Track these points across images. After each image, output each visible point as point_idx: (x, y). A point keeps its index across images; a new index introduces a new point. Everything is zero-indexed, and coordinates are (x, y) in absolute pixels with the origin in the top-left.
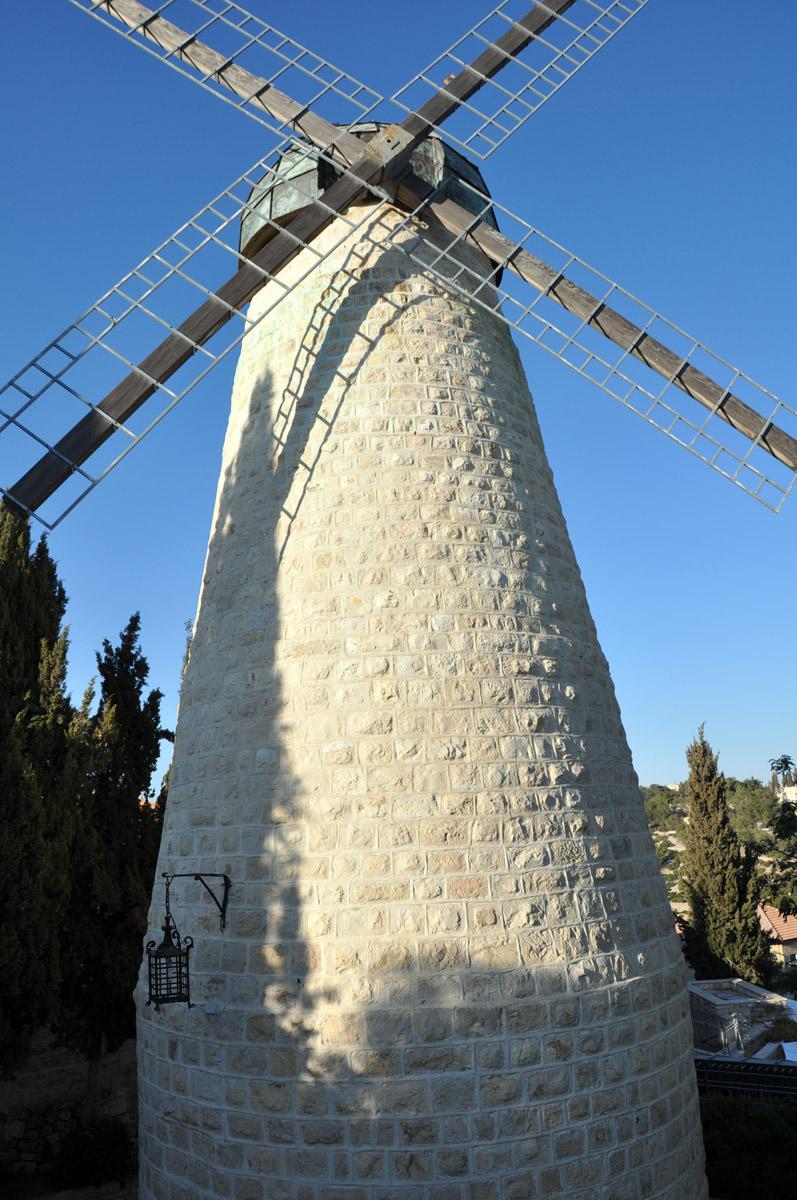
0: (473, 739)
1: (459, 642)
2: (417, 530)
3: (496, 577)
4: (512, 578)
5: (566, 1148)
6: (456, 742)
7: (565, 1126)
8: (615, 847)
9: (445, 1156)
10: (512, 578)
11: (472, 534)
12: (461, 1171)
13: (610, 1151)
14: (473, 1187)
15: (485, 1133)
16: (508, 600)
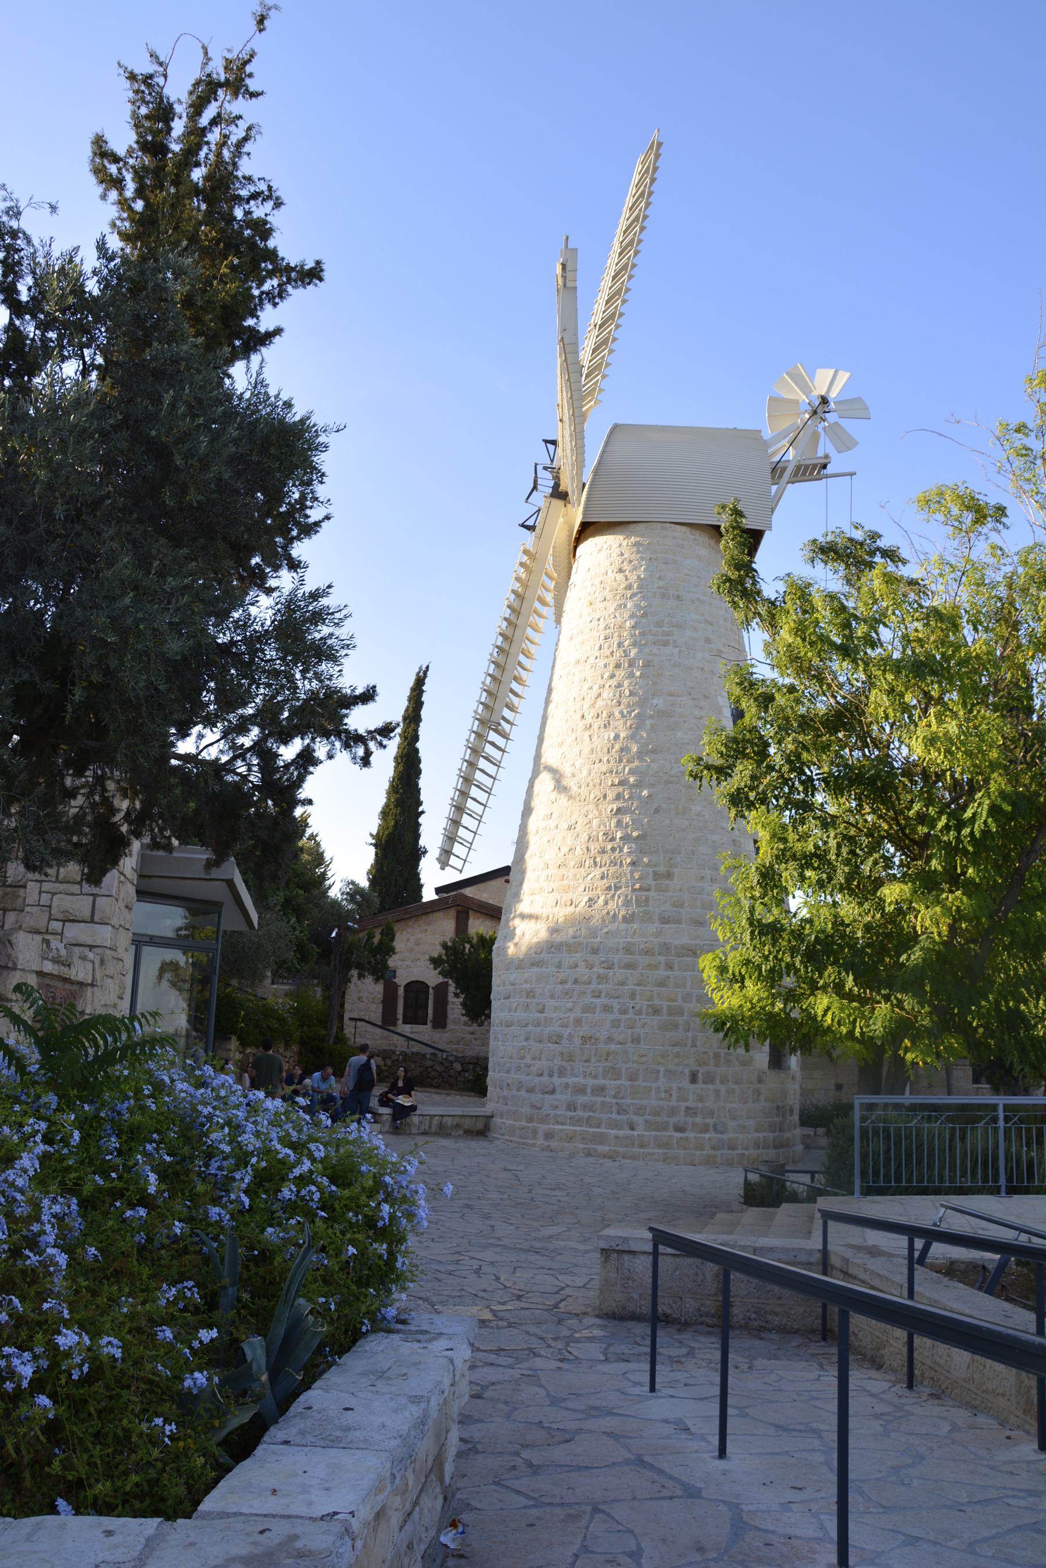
0: (580, 821)
1: (585, 772)
2: (578, 716)
3: (612, 735)
4: (622, 735)
5: (589, 1009)
6: (573, 822)
7: (588, 999)
8: (655, 874)
9: (538, 1004)
10: (622, 735)
11: (604, 715)
12: (542, 1011)
13: (611, 1017)
14: (546, 1018)
15: (552, 997)
16: (617, 747)
